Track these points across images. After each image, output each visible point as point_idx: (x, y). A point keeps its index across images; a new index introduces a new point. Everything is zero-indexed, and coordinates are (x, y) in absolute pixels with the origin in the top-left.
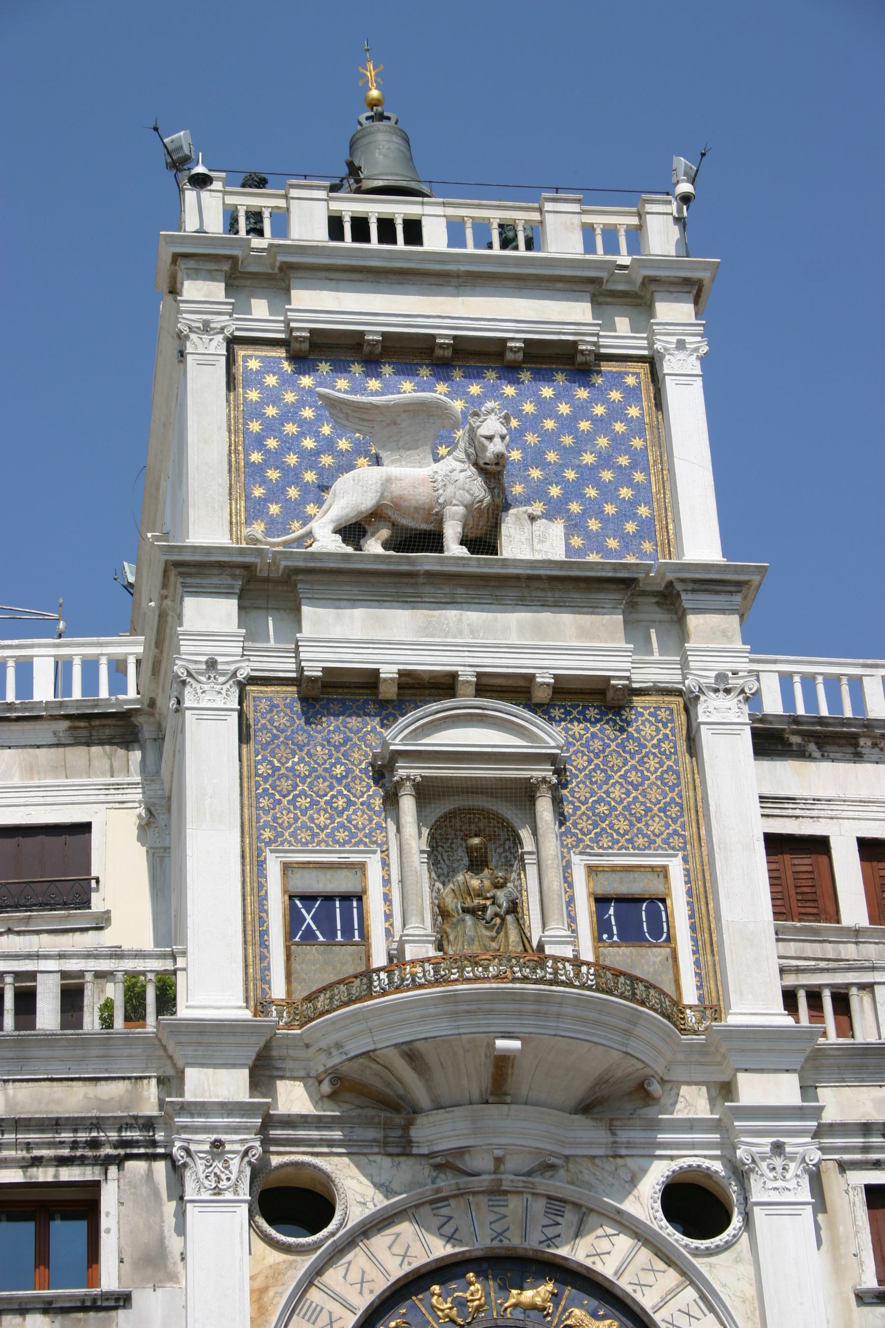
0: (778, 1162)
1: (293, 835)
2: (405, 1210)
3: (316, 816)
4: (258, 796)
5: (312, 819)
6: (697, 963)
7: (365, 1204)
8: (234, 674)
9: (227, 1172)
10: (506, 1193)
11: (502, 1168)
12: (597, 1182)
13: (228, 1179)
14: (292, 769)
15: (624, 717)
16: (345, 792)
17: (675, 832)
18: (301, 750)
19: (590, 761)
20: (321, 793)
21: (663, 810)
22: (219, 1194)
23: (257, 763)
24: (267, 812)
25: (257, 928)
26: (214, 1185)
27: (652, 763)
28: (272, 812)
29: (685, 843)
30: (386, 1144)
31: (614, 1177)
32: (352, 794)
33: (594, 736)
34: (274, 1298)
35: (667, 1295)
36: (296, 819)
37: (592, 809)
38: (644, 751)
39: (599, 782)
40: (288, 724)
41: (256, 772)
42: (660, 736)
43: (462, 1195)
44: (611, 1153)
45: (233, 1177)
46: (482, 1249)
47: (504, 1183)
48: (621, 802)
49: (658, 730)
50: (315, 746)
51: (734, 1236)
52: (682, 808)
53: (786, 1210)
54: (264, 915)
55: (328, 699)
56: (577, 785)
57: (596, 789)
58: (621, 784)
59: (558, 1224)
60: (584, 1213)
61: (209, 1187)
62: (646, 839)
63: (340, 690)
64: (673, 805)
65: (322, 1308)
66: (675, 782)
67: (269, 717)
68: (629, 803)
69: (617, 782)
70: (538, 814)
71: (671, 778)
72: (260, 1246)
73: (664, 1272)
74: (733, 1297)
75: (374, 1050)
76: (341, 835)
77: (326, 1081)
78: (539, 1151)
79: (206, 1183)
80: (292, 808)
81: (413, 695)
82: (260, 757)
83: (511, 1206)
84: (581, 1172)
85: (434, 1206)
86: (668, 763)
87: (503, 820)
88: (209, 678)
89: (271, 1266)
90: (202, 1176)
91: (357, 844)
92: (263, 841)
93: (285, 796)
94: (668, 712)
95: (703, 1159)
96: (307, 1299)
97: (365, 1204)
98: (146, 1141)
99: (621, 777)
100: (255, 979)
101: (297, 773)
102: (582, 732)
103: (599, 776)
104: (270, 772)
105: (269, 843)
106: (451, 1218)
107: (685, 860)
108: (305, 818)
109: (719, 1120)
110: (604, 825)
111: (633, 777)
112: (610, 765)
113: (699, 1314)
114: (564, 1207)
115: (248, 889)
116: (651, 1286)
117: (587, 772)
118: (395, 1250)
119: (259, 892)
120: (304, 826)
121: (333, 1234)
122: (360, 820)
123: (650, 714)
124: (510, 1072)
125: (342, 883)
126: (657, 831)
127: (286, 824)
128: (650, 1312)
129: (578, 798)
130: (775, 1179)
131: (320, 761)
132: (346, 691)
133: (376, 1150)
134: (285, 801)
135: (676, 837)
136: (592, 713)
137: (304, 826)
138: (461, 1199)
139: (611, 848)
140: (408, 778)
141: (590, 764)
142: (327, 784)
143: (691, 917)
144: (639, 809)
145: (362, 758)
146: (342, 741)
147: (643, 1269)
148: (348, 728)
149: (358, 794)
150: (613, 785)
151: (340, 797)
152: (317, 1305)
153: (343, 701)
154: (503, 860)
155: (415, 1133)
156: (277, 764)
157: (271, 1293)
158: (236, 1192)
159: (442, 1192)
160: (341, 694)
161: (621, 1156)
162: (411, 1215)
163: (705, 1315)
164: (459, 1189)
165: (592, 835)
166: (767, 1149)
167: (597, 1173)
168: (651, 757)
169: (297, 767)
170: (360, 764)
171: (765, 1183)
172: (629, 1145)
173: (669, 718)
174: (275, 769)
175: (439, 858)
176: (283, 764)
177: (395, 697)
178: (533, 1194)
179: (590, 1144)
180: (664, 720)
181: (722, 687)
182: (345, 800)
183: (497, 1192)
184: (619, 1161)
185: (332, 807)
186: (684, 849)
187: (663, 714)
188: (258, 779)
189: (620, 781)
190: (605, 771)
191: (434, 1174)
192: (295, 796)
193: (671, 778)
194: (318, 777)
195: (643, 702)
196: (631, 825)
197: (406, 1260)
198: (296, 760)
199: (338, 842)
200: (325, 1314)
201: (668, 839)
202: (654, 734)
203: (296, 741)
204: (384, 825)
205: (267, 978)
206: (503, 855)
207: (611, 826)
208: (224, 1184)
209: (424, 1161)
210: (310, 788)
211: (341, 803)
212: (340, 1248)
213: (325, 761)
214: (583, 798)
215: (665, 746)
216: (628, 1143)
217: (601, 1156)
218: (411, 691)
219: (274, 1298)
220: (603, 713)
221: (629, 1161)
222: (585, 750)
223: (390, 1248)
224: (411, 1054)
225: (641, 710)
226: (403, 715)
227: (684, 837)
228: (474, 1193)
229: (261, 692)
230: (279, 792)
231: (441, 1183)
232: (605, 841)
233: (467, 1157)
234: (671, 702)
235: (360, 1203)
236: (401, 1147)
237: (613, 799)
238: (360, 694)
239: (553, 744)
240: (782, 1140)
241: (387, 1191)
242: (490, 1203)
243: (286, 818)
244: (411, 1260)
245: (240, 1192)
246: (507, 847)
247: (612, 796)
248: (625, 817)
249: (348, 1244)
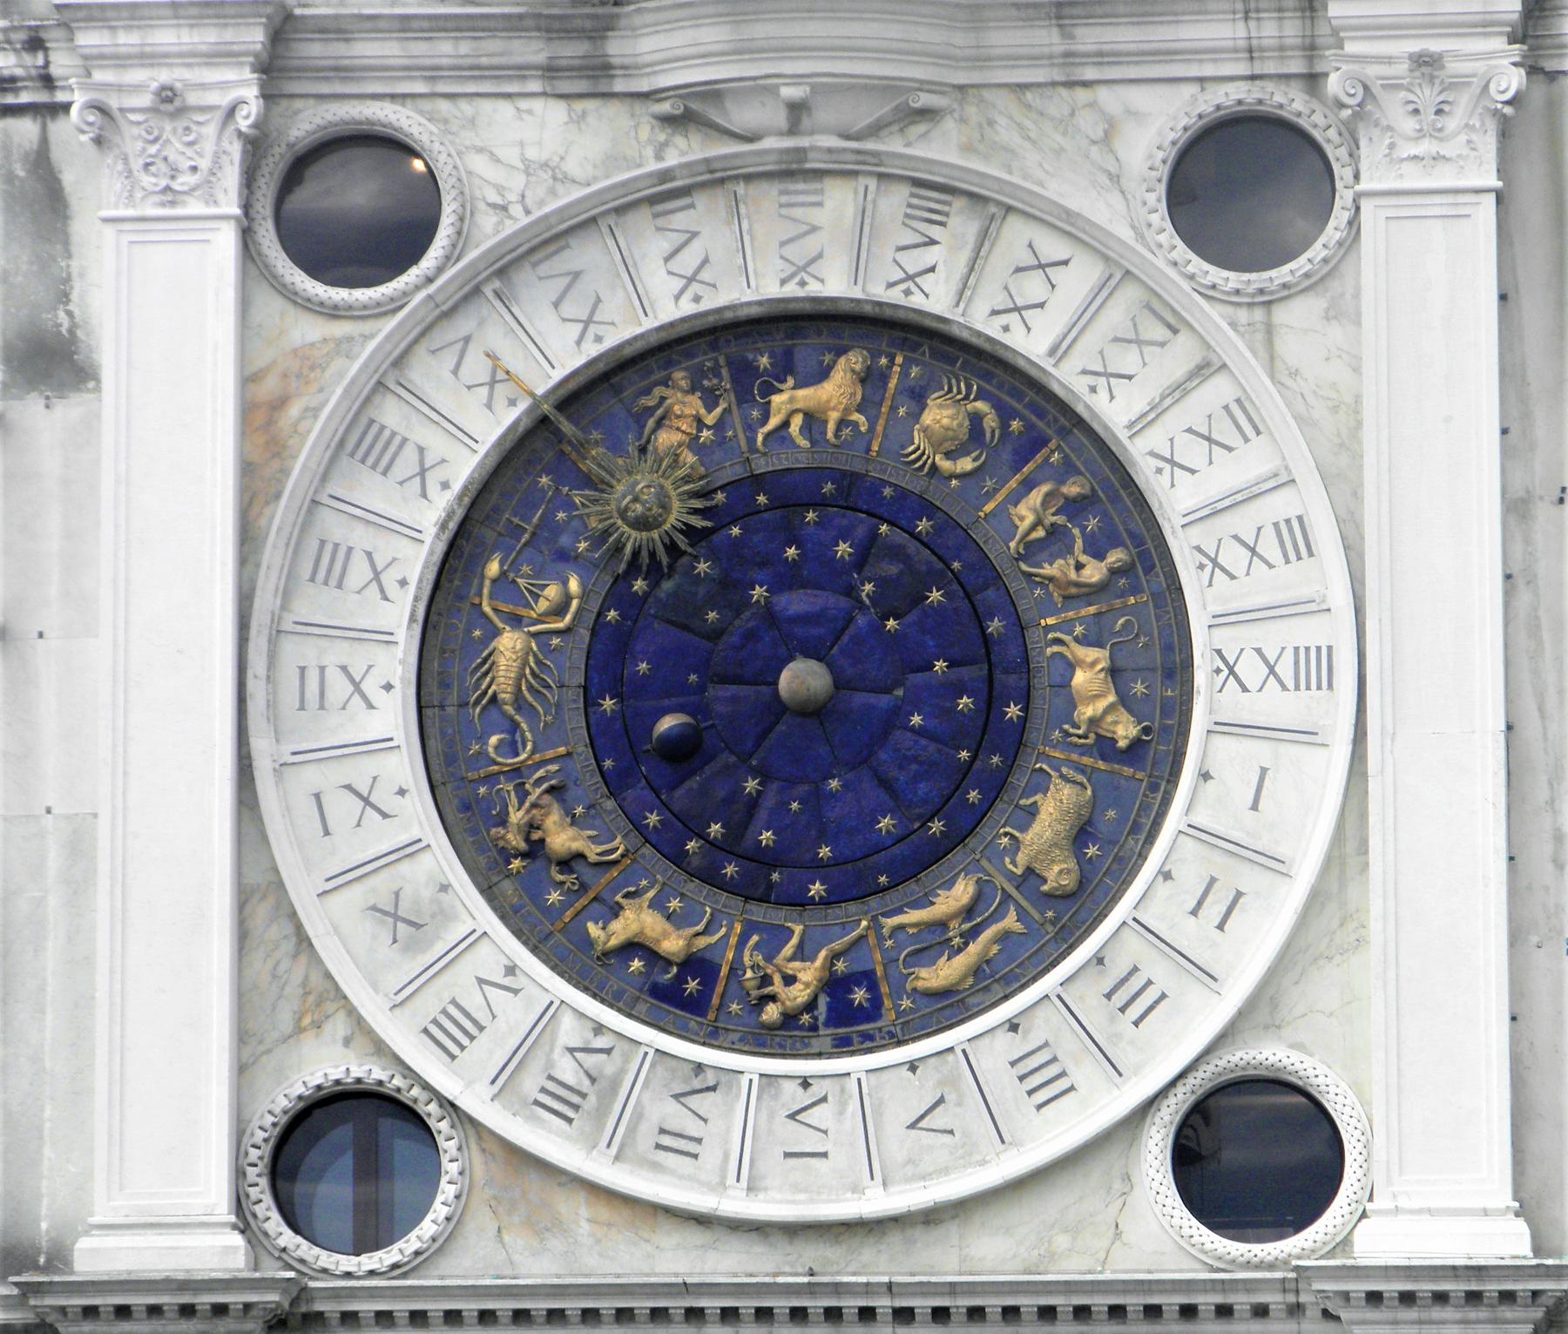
0: (1427, 96)
2: (593, 220)
7: (504, 208)
9: (189, 152)
10: (819, 174)
11: (806, 122)
12: (1027, 145)
13: (194, 169)
22: (173, 203)
26: (163, 183)
30: (550, 70)
31: (1065, 134)
34: (302, 418)
35: (1163, 398)
43: (722, 181)
44: (1063, 79)
45: (204, 164)
46: (760, 303)
47: (811, 155)
51: (1325, 261)
53: (1437, 206)
59: (933, 242)
60: (993, 217)
61: (151, 188)
65: (405, 440)
72: (269, 306)
73: (1162, 344)
74: (1311, 399)
78: (888, 87)
79: (147, 180)
83: (829, 204)
84: (991, 123)
85: (659, 208)
89: (295, 351)
90: (137, 164)
95: (1270, 86)
96: (372, 421)
97: (504, 208)
98: (30, 78)
106: (695, 234)
113: (1233, 439)
114: (950, 204)
116: (1130, 378)
118: (568, 309)
121: (430, 280)
128: (1123, 435)
130: (1420, 135)
133: (534, 86)
138: (719, 191)
147: (1116, 340)
152: (394, 434)
155: (616, 48)
157: (294, 410)
158: (212, 200)
159: (673, 179)
161: (1086, 84)
162: (605, 230)
163: (1247, 440)
164: (711, 172)
166: (1402, 68)
167: (1028, 123)
171: (1392, 146)
172: (1101, 57)
178: (881, 177)
179: (1014, 60)
183: (794, 171)
184: (1082, 95)
191: (662, 137)
197: (592, 329)
200: (409, 454)
208: (185, 180)
209: (639, 107)
212: (444, 308)
216: (1100, 54)
217: (1039, 85)
219: (302, 418)
221: (1104, 95)
223: (556, 305)
228: (749, 178)
231: (672, 160)
233: (729, 104)
235: (494, 206)
236: (591, 80)
240: (1435, 46)
241: (555, 178)
242: (784, 199)
244: (601, 330)
245: (221, 197)
249: (466, 299)
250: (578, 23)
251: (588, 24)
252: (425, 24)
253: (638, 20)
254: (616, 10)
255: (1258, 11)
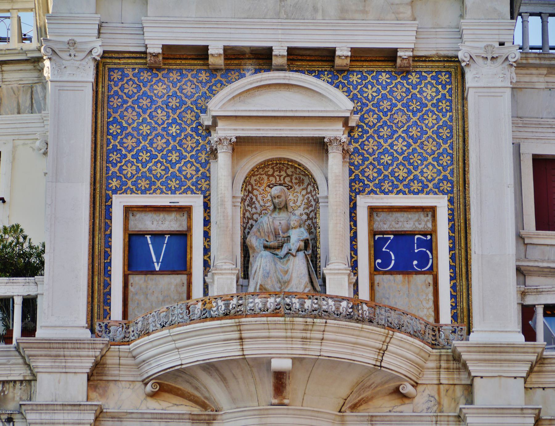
1: (135, 184)
3: (154, 168)
4: (109, 152)
5: (150, 170)
6: (454, 287)
8: (91, 51)
14: (137, 129)
15: (410, 81)
16: (178, 148)
17: (445, 177)
18: (144, 112)
19: (379, 119)
20: (159, 148)
21: (436, 159)
23: (108, 123)
24: (114, 165)
25: (102, 261)
27: (430, 120)
28: (119, 165)
29: (452, 187)
32: (184, 148)
33: (384, 97)
36: (138, 170)
37: (378, 160)
38: (424, 109)
39: (385, 136)
40: (135, 91)
41: (108, 131)
42: (439, 97)
48: (403, 153)
49: (438, 92)
50: (155, 110)
52: (452, 157)
54: (108, 250)
55: (169, 69)
56: (367, 140)
57: (382, 143)
58: (404, 139)
62: (420, 184)
63: (178, 62)
64: (445, 156)
66: (448, 135)
67: (120, 85)
68: (409, 154)
69: (400, 136)
70: (329, 167)
71: (445, 133)
75: (182, 365)
76: (173, 184)
77: (149, 385)
80: (135, 161)
81: (237, 65)
82: (111, 119)
86: (444, 119)
87: (306, 169)
88: (70, 55)
91: (185, 192)
92: (111, 189)
93: (130, 152)
94: (447, 76)
99: (404, 132)
100: (99, 301)
101: (141, 132)
102: (375, 94)
103: (385, 132)
104: (119, 131)
105: (115, 192)
107: (451, 201)
108: (145, 170)
109: (459, 416)
110: (386, 173)
111: (414, 132)
112: (396, 121)
115: (97, 228)
117: (376, 128)
119: (105, 230)
120: (144, 176)
122: (190, 171)
123: (433, 78)
124: (287, 382)
125: (170, 223)
126: (430, 177)
127: (129, 175)
129: (367, 151)
131: (160, 122)
132: (183, 62)
134: (129, 156)
135: (445, 183)
136: (384, 77)
137: (144, 176)
139: (391, 192)
140: (226, 138)
141: (379, 122)
142: (164, 140)
143: (451, 249)
144: (416, 159)
145: (194, 119)
146: (178, 105)
148: (184, 94)
149: (189, 149)
150: (397, 139)
151: (174, 152)
153: (180, 70)
154: (306, 201)
156: (125, 125)
160: (179, 65)
165: (377, 182)
168: (430, 114)
169: (141, 127)
170: (192, 124)
173: (448, 80)
174: (123, 129)
175: (254, 200)
176: (130, 125)
177: (223, 67)
180: (444, 82)
181: (489, 57)
182: (177, 154)
185: (167, 160)
186: (451, 192)
187: (444, 78)
188: (109, 137)
189: (403, 135)
190: (390, 127)
192: (138, 151)
193: (445, 133)
194: (157, 135)
195: (427, 67)
196: (409, 172)
198: (140, 121)
199: (170, 189)
201: (439, 183)
202: (434, 94)
203: (141, 105)
204: (208, 175)
205: (108, 301)
206: (307, 196)
207: (393, 173)
210: (151, 145)
211: (174, 157)
213: (164, 122)
214: (371, 151)
215: (443, 105)
218: (236, 62)
220: (393, 78)
222: (376, 109)
224: (210, 367)
225: (426, 75)
226: (230, 82)
227: (452, 182)
229: (115, 64)
230: (126, 148)
232: (386, 186)
234: (449, 67)
237: (396, 151)
238: (195, 65)
239: (344, 108)
243: (130, 170)
246: (309, 190)
247: (395, 148)
248: (404, 165)
250: (203, 417)
251: (207, 418)
252: (150, 416)
253: (224, 417)
254: (217, 413)
255: (440, 421)
